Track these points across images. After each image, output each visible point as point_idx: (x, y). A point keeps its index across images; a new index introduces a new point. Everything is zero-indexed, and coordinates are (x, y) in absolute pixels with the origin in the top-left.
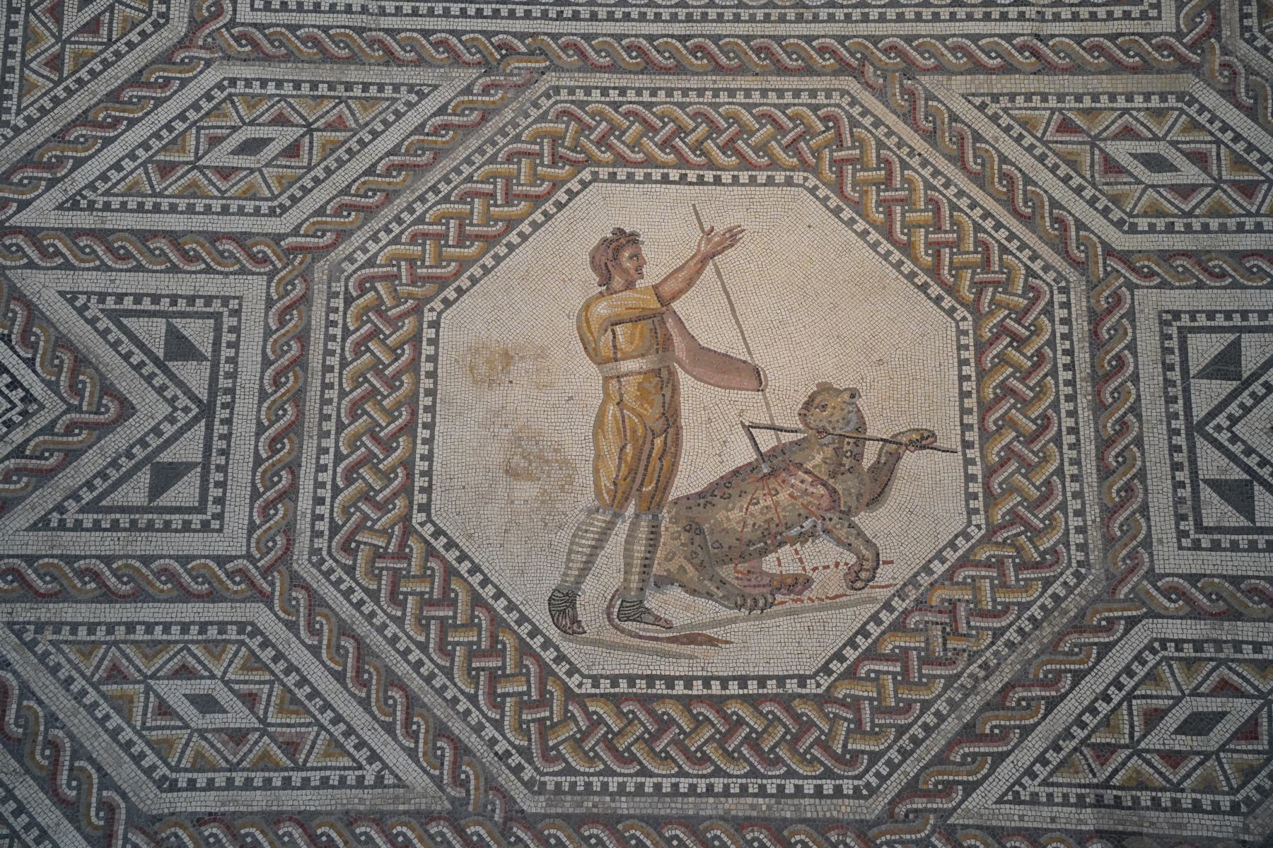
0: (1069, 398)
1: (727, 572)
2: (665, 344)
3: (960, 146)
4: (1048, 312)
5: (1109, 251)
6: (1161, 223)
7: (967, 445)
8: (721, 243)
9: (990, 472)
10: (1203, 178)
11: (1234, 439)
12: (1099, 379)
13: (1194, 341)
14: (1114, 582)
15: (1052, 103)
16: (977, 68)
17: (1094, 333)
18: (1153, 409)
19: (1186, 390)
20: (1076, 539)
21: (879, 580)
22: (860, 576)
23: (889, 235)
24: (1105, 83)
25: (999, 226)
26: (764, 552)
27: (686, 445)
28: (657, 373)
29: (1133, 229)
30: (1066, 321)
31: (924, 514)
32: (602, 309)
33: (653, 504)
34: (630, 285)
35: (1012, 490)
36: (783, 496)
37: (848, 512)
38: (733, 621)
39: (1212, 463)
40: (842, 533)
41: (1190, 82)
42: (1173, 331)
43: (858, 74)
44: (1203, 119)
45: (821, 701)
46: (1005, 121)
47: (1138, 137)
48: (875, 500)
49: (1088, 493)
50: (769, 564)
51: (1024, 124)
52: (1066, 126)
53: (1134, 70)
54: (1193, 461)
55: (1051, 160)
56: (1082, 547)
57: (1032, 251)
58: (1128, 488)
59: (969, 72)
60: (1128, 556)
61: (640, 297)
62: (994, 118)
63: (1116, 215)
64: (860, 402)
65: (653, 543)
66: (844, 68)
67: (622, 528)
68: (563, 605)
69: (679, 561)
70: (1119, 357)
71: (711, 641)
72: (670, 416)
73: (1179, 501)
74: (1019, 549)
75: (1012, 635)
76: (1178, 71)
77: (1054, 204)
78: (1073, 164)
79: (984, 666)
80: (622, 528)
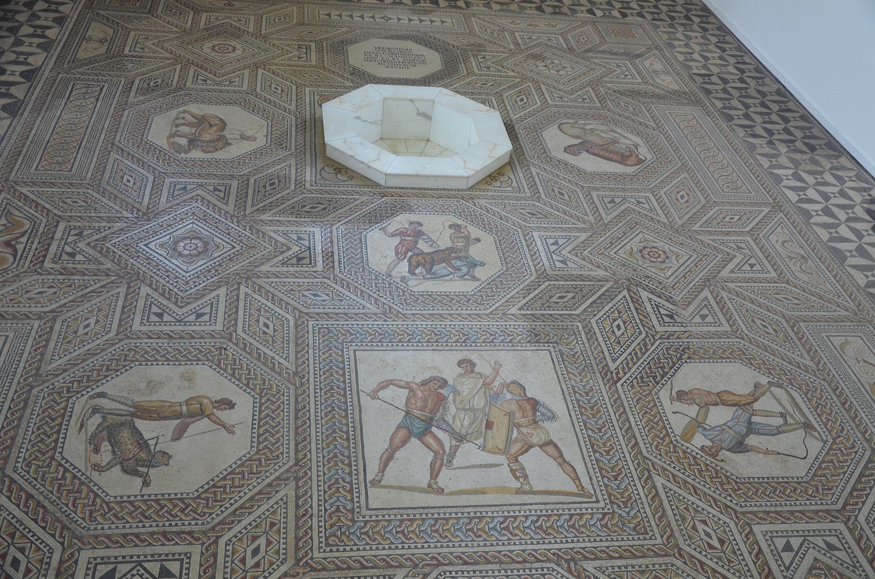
0: (157, 526)
1: (105, 433)
2: (191, 416)
3: (265, 493)
4: (194, 519)
5: (218, 537)
6: (229, 553)
7: (142, 496)
8: (230, 430)
9: (131, 503)
10: (248, 566)
11: (133, 575)
12: (164, 534)
13: (178, 564)
14: (80, 539)
15: (283, 520)
16: (298, 498)
17: (184, 533)
18: (149, 550)
19: (156, 561)
20: (99, 527)
21: (94, 472)
22: (97, 467)
23: (229, 474)
24: (291, 536)
25: (231, 504)
26: (110, 442)
27: (153, 422)
28: (181, 414)
29: (227, 545)
30: (190, 524)
31: (117, 484)
32: (206, 401)
33: (133, 415)
34: (214, 407)
35: (122, 509)
36: (130, 446)
37: (121, 463)
38: (86, 435)
39: (123, 569)
40: (114, 462)
41: (291, 562)
42: (182, 557)
43: (296, 464)
44: (274, 566)
45: (52, 458)
46: (276, 506)
47: (267, 546)
48: (125, 471)
49: (117, 529)
50: (106, 443)
51: (274, 512)
52: (272, 525)
53: (297, 545)
54: (125, 562)
55: (259, 520)
56: (96, 529)
57: (218, 515)
58: (117, 542)
59: (296, 496)
60: (89, 542)
61: (209, 409)
62: (277, 503)
63: (234, 540)
64: (164, 466)
65: (117, 415)
66: (297, 461)
67: (126, 408)
68: (102, 395)
69: (111, 421)
70: (173, 540)
71: (81, 429)
72: (165, 418)
73: (109, 558)
74: (98, 511)
75: (65, 508)
76: (296, 559)
77: (239, 521)
78: (257, 526)
79: (55, 501)
80: (126, 408)
